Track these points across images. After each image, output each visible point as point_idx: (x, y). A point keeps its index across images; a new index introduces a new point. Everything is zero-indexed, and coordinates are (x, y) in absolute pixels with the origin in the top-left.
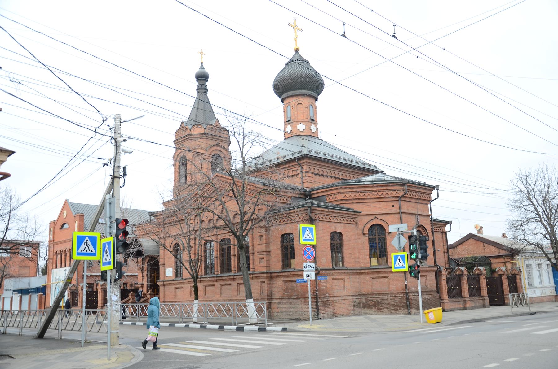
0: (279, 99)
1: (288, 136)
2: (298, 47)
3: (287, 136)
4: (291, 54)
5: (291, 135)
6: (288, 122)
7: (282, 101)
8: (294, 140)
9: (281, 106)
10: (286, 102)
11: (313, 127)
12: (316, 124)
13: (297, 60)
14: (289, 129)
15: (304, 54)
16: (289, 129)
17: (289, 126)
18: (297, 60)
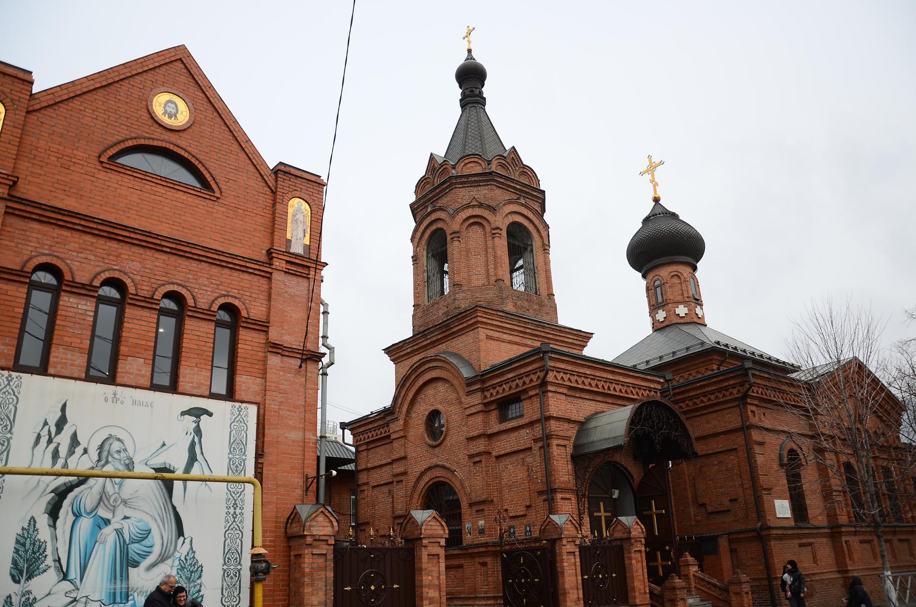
0: (640, 275)
1: (658, 328)
2: (660, 194)
3: (659, 326)
4: (647, 208)
5: (664, 324)
6: (654, 308)
7: (644, 276)
8: (672, 333)
9: (644, 283)
10: (651, 276)
11: (698, 310)
12: (701, 305)
13: (659, 214)
14: (661, 315)
15: (668, 204)
16: (661, 315)
17: (660, 311)
18: (659, 214)
